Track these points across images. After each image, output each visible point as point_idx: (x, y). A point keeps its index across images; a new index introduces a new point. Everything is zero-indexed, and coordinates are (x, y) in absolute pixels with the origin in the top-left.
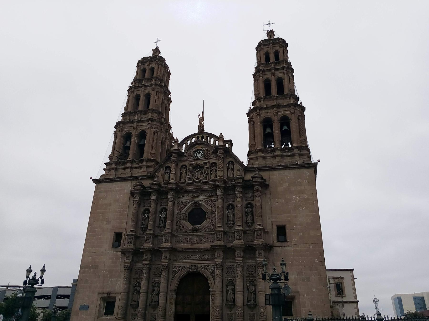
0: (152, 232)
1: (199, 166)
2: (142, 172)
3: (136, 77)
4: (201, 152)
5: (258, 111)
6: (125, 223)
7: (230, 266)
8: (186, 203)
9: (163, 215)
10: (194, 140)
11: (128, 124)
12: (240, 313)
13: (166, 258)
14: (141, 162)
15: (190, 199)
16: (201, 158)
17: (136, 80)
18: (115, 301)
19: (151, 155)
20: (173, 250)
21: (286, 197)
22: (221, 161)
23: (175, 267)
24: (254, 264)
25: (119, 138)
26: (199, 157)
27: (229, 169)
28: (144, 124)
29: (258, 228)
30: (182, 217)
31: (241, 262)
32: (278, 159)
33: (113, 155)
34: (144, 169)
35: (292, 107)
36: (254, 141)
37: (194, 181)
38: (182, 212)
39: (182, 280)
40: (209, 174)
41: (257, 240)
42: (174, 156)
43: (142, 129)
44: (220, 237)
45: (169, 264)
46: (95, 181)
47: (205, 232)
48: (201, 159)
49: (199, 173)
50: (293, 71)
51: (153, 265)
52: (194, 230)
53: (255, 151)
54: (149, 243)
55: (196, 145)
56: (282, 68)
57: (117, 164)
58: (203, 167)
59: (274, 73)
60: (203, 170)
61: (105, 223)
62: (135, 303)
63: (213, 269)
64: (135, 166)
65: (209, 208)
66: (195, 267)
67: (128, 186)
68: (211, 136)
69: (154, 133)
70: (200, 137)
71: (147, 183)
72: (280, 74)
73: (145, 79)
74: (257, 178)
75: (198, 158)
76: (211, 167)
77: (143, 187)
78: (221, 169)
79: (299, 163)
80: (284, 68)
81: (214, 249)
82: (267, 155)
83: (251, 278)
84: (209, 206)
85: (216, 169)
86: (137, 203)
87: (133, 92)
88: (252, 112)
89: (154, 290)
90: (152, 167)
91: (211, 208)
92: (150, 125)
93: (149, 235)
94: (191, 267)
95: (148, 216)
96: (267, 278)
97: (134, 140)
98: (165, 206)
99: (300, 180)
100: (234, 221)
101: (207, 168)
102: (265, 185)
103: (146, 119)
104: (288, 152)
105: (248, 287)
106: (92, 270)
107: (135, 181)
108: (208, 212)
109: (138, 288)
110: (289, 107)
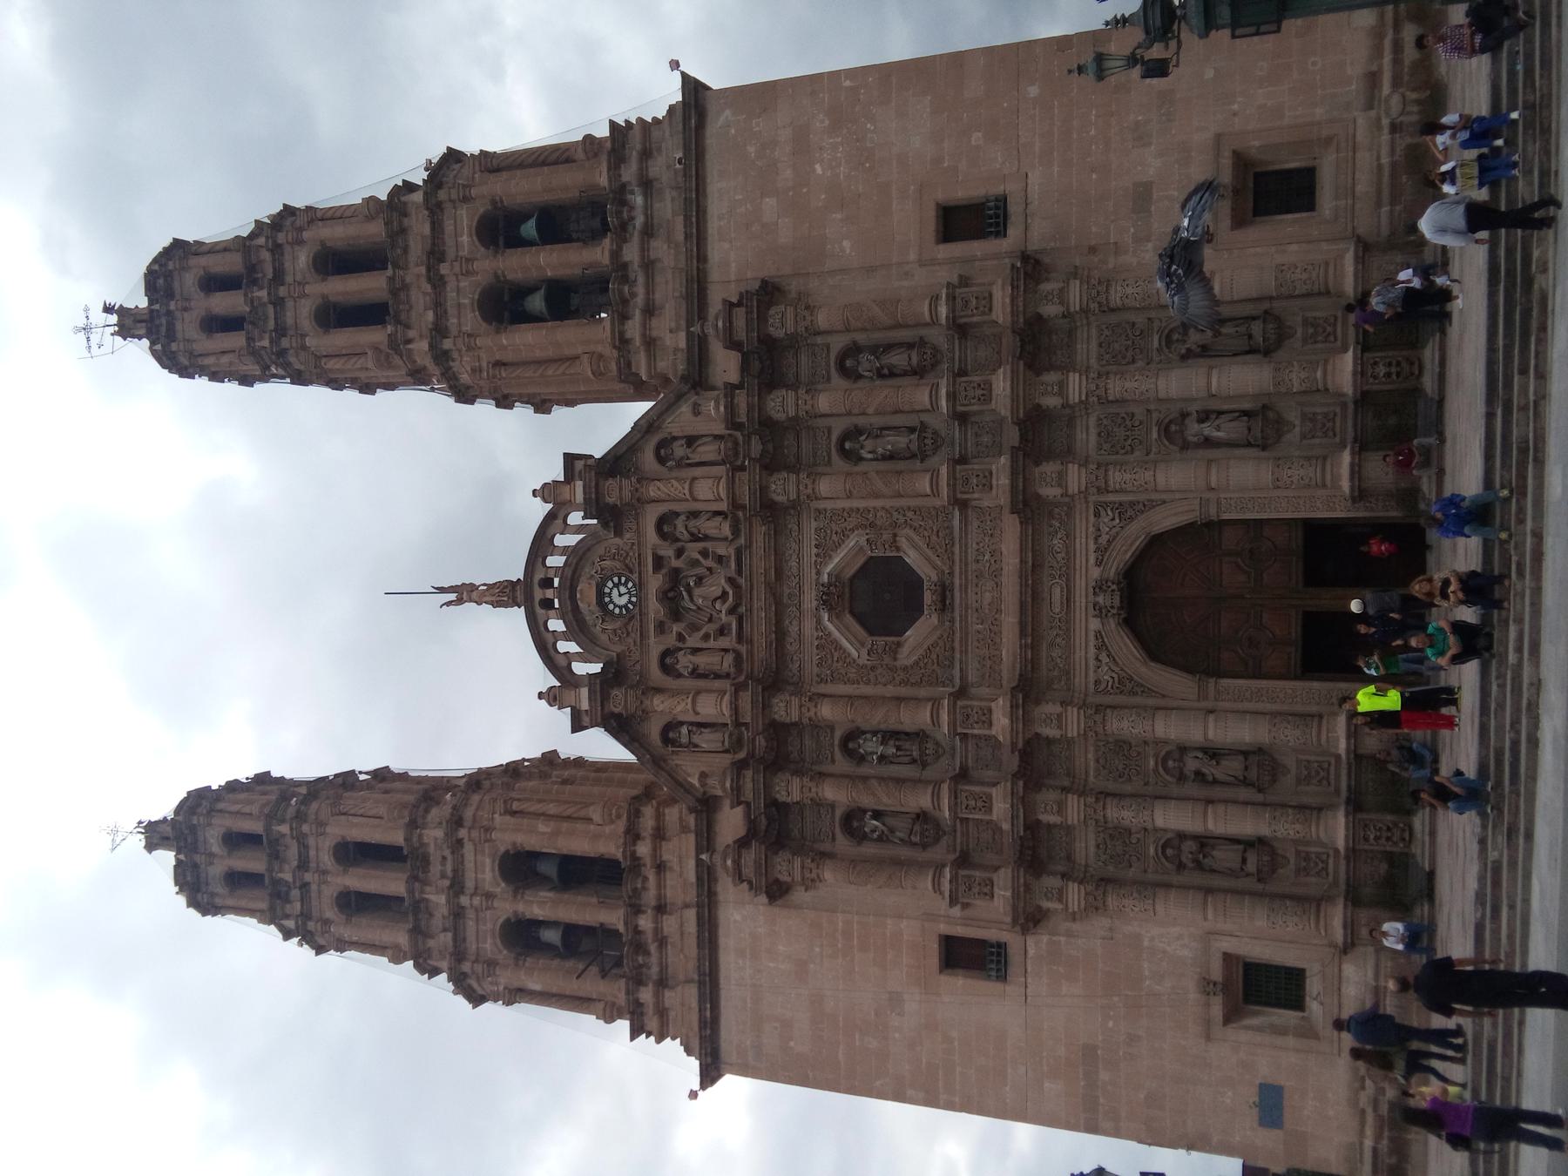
0: (945, 787)
1: (671, 595)
2: (682, 854)
3: (258, 914)
4: (610, 584)
5: (447, 344)
6: (902, 926)
7: (1099, 434)
8: (826, 644)
9: (871, 746)
10: (556, 625)
11: (464, 940)
12: (1303, 375)
13: (1059, 716)
14: (636, 862)
15: (808, 626)
16: (634, 585)
17: (270, 916)
18: (1241, 965)
19: (612, 822)
20: (1027, 690)
21: (820, 204)
22: (653, 491)
23: (1097, 682)
24: (1094, 332)
25: (523, 977)
27: (688, 458)
28: (469, 864)
29: (943, 311)
30: (887, 660)
31: (1084, 382)
32: (659, 248)
33: (600, 1001)
34: (669, 853)
35: (442, 195)
36: (578, 362)
37: (731, 611)
38: (864, 659)
39: (1154, 652)
40: (705, 548)
41: (994, 313)
42: (620, 700)
43: (493, 870)
44: (978, 476)
45: (1083, 706)
46: (709, 1076)
47: (953, 553)
48: (640, 586)
49: (697, 592)
50: (288, 211)
51: (1086, 780)
52: (944, 605)
53: (619, 349)
54: (990, 797)
55: (576, 609)
56: (276, 249)
57: (638, 981)
58: (676, 572)
59: (292, 288)
60: (687, 577)
62: (1252, 859)
63: (1112, 509)
64: (650, 897)
65: (851, 543)
66: (1100, 588)
67: (738, 917)
68: (541, 544)
69: (514, 813)
70: (544, 594)
71: (731, 823)
72: (300, 260)
73: (270, 870)
74: (731, 323)
75: (634, 599)
76: (678, 540)
77: (742, 843)
78: (687, 486)
79: (679, 155)
80: (274, 242)
81: (1027, 506)
82: (640, 300)
83: (1156, 344)
84: (843, 541)
85: (688, 518)
86: (813, 861)
87: (327, 922)
88: (450, 372)
89: (1198, 773)
90: (664, 815)
91: (852, 530)
92: (475, 834)
93: (956, 798)
94: (1100, 610)
95: (877, 815)
96: (1157, 52)
97: (540, 905)
98: (836, 742)
99: (751, 149)
100: (912, 430)
101: (679, 553)
102: (768, 293)
103: (450, 857)
104: (632, 208)
105: (1194, 347)
107: (719, 889)
108: (867, 540)
109: (1189, 846)
110: (442, 210)
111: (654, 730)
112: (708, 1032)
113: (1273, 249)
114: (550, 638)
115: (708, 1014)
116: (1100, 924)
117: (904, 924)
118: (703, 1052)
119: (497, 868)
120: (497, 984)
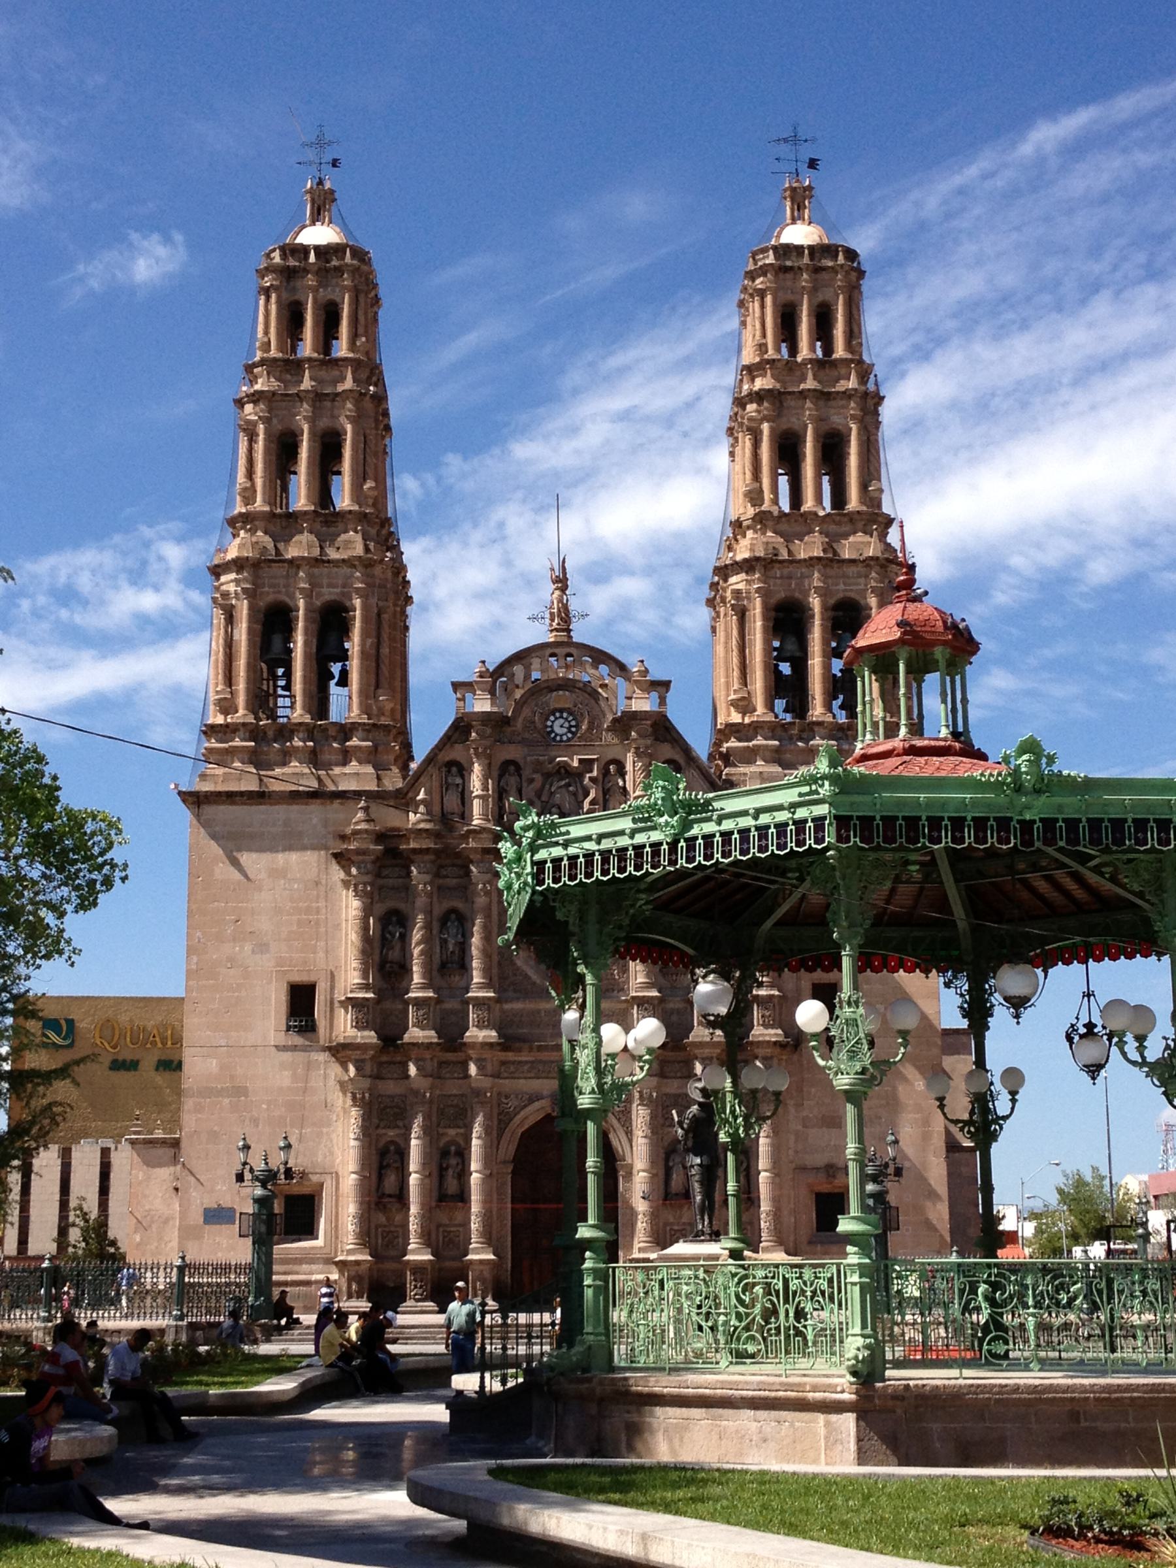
1: (563, 771)
16: (569, 740)
23: (507, 1097)
26: (561, 736)
43: (330, 593)
49: (564, 790)
61: (248, 948)
67: (315, 821)
68: (600, 657)
69: (379, 615)
75: (558, 738)
111: (456, 753)
113: (792, 1206)
114: (524, 662)
116: (341, 1101)
117: (321, 955)
119: (333, 597)
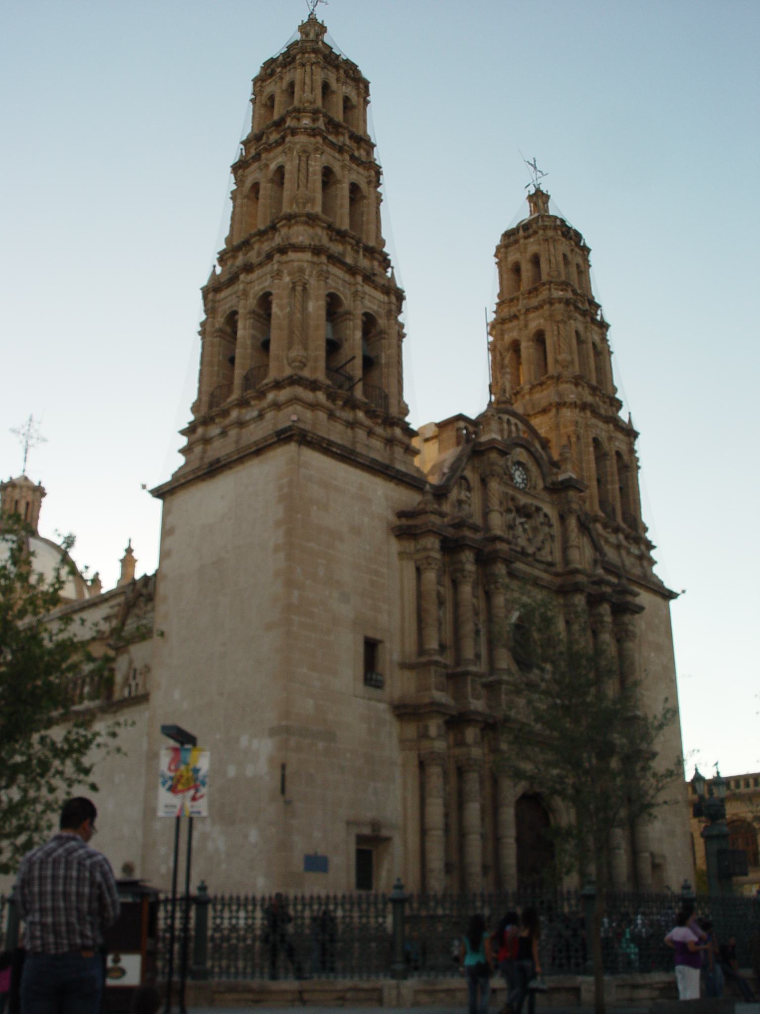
43: (370, 308)
106: (321, 745)
112: (324, 445)
115: (334, 450)
118: (315, 437)
120: (310, 276)
